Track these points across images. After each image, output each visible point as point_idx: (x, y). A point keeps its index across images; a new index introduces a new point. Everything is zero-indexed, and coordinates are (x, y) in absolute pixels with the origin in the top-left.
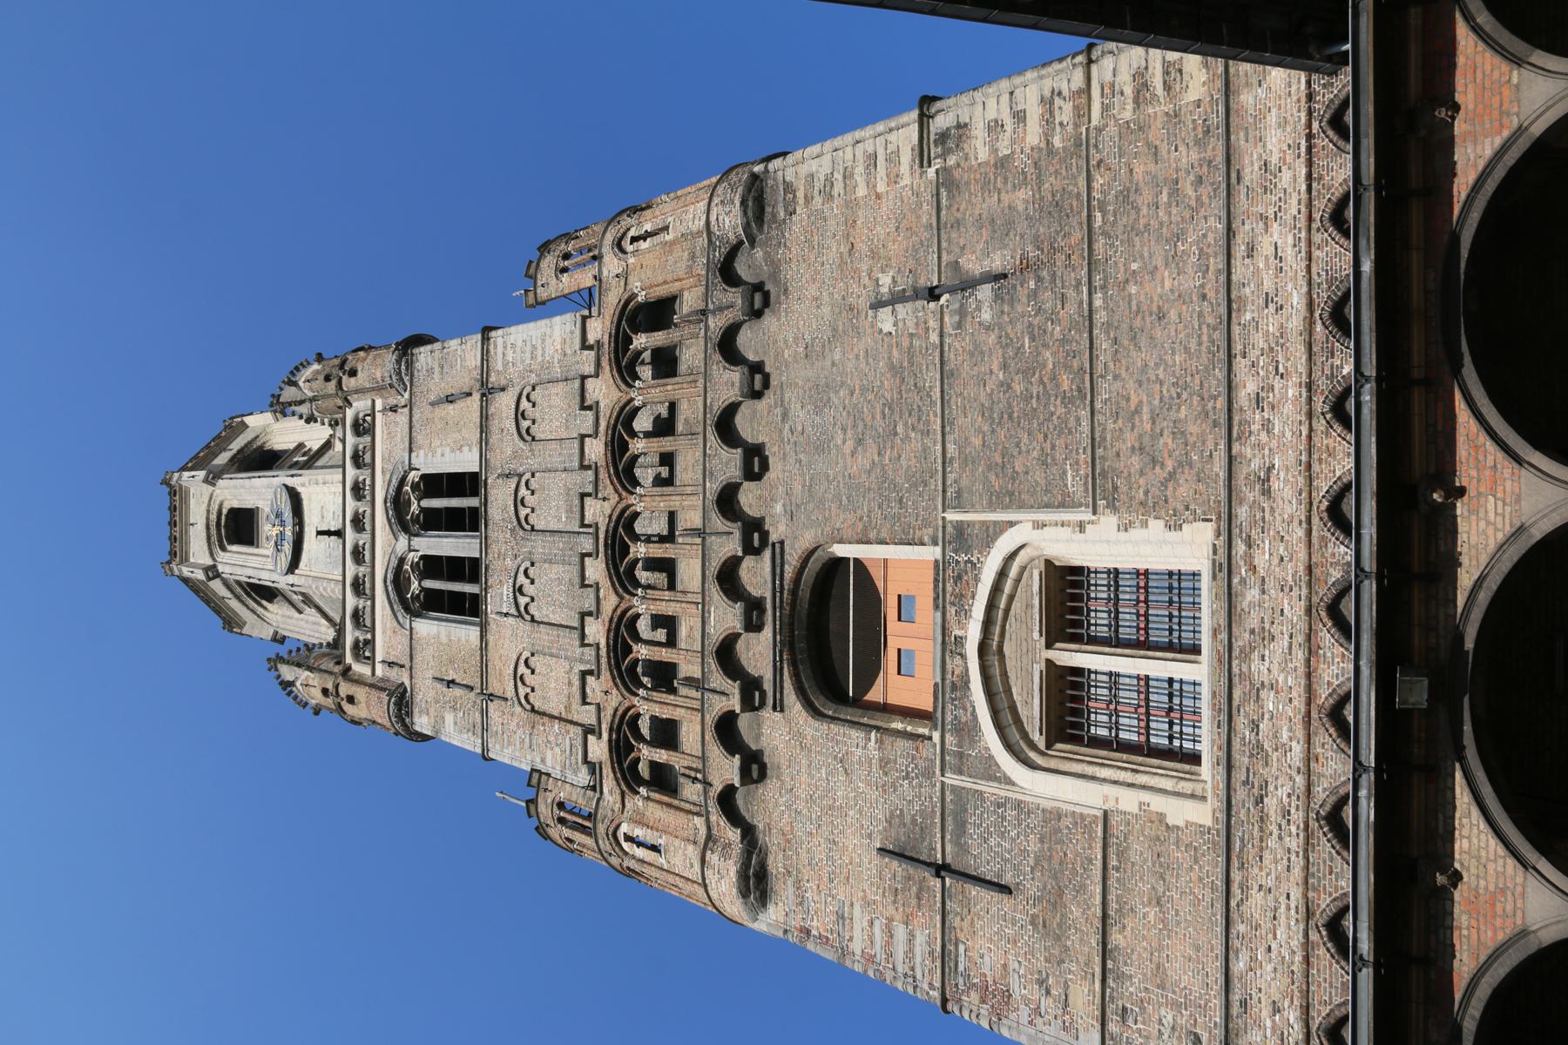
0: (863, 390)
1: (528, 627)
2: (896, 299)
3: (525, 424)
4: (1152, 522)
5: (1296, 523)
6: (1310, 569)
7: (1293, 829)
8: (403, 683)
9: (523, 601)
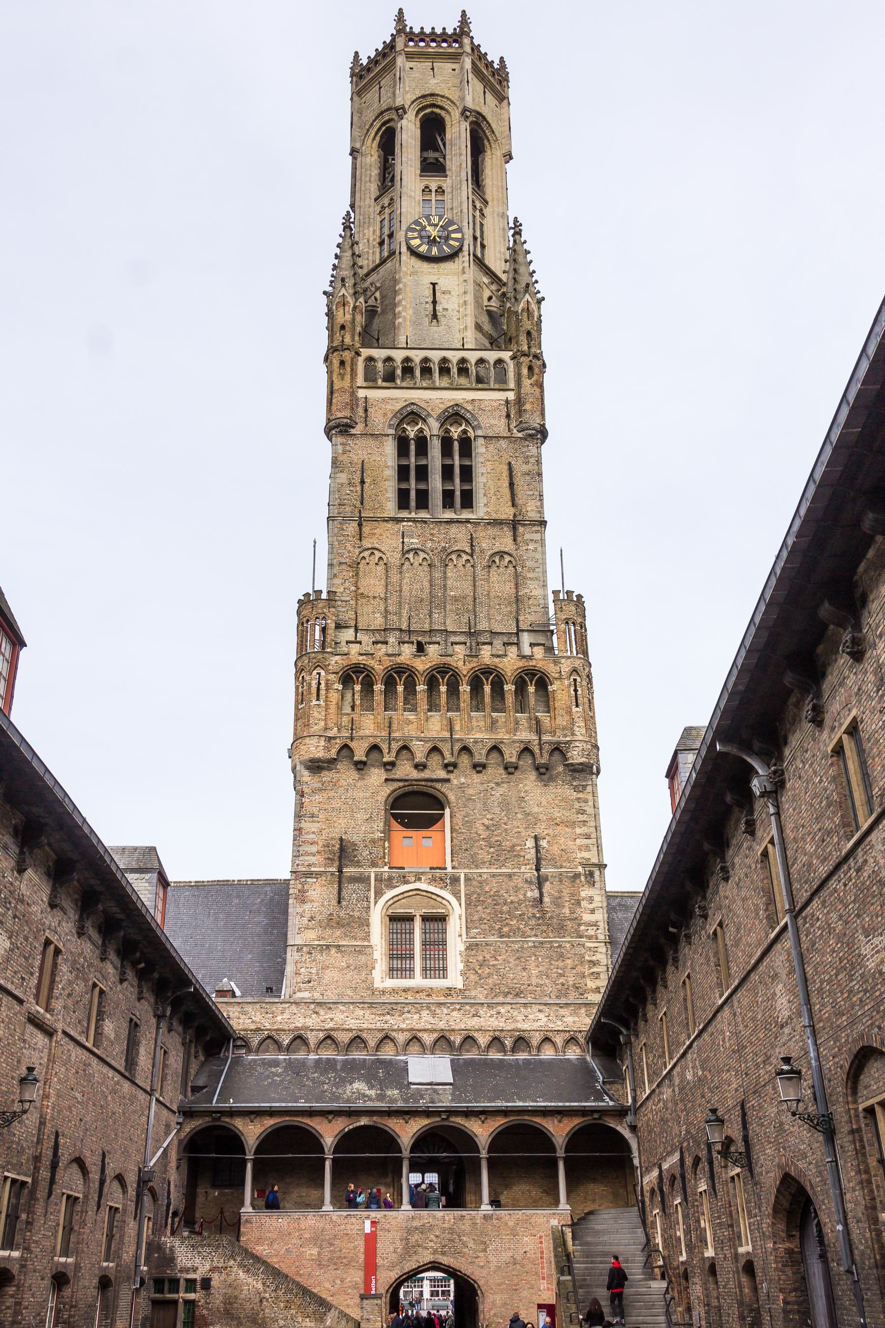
0: (506, 830)
1: (398, 563)
2: (537, 847)
3: (497, 559)
4: (463, 964)
6: (453, 1030)
8: (357, 424)
9: (411, 556)
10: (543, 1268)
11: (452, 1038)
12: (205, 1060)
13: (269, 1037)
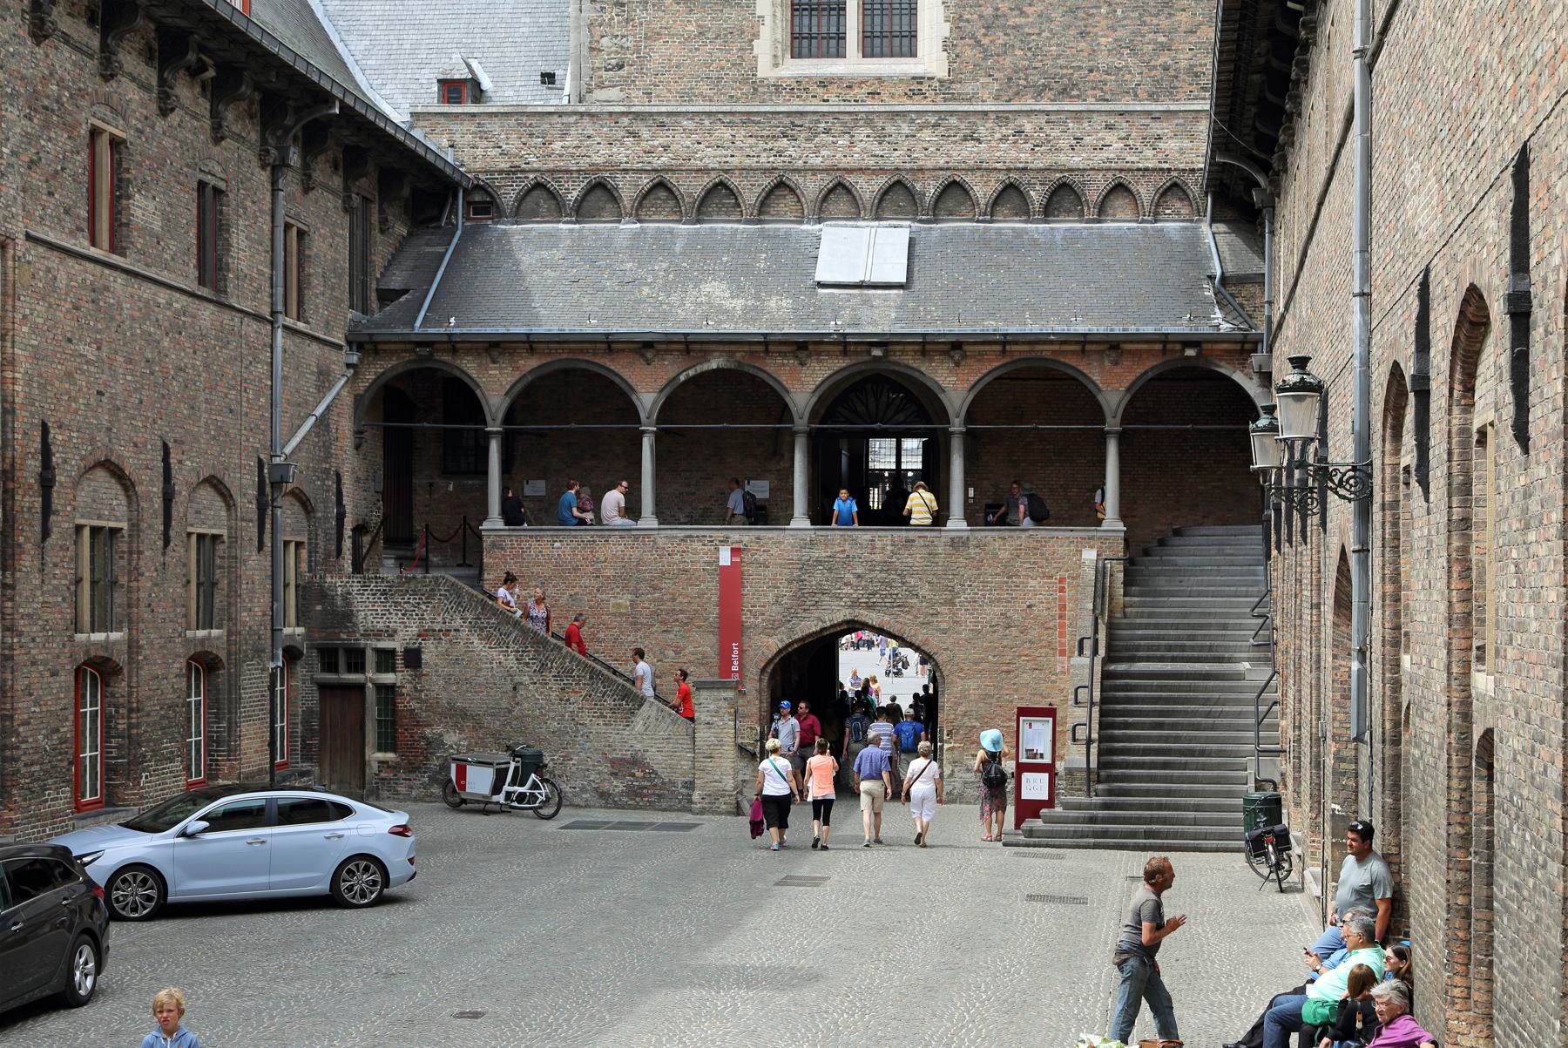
5: (947, 159)
6: (921, 170)
7: (772, 159)
10: (1062, 635)
11: (918, 186)
12: (410, 234)
13: (539, 186)
